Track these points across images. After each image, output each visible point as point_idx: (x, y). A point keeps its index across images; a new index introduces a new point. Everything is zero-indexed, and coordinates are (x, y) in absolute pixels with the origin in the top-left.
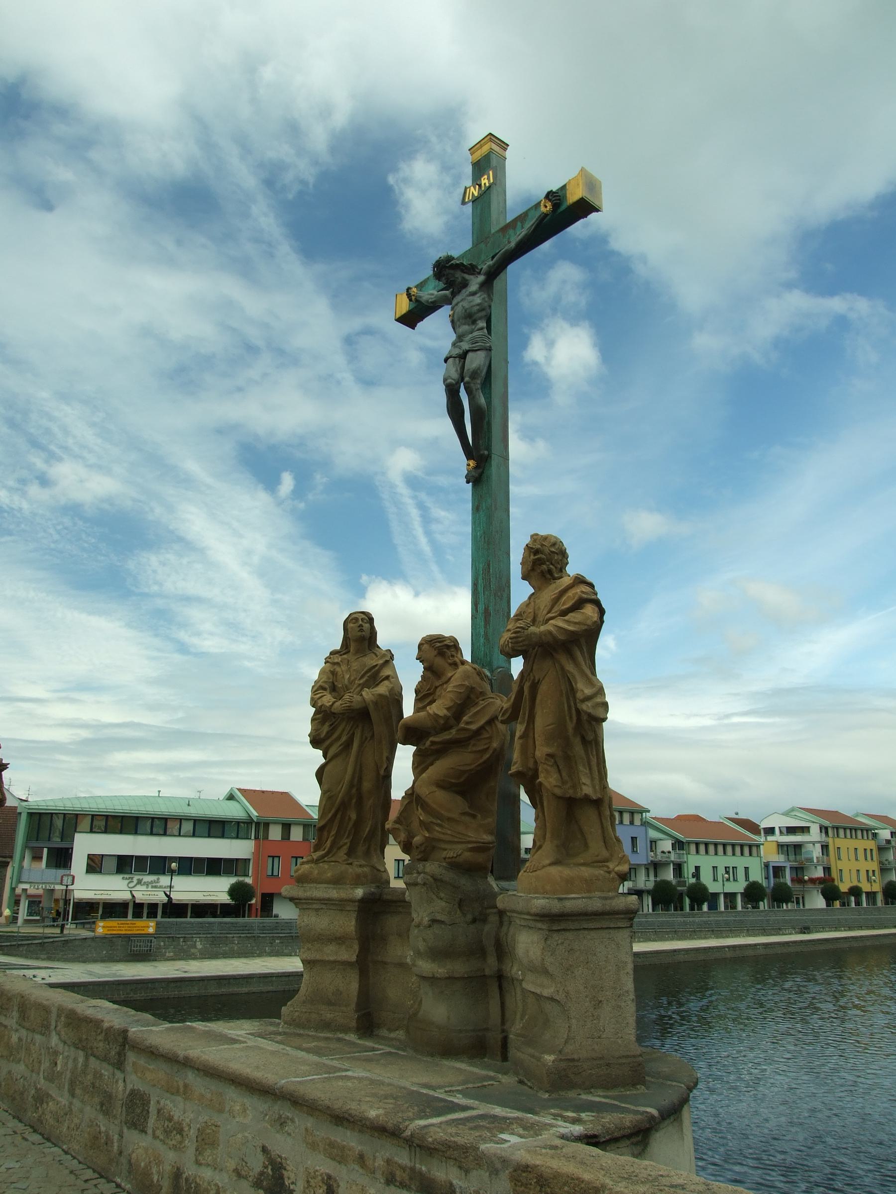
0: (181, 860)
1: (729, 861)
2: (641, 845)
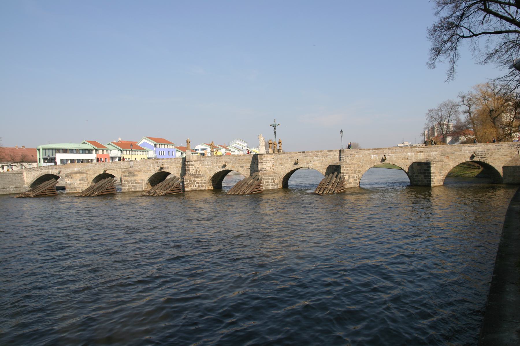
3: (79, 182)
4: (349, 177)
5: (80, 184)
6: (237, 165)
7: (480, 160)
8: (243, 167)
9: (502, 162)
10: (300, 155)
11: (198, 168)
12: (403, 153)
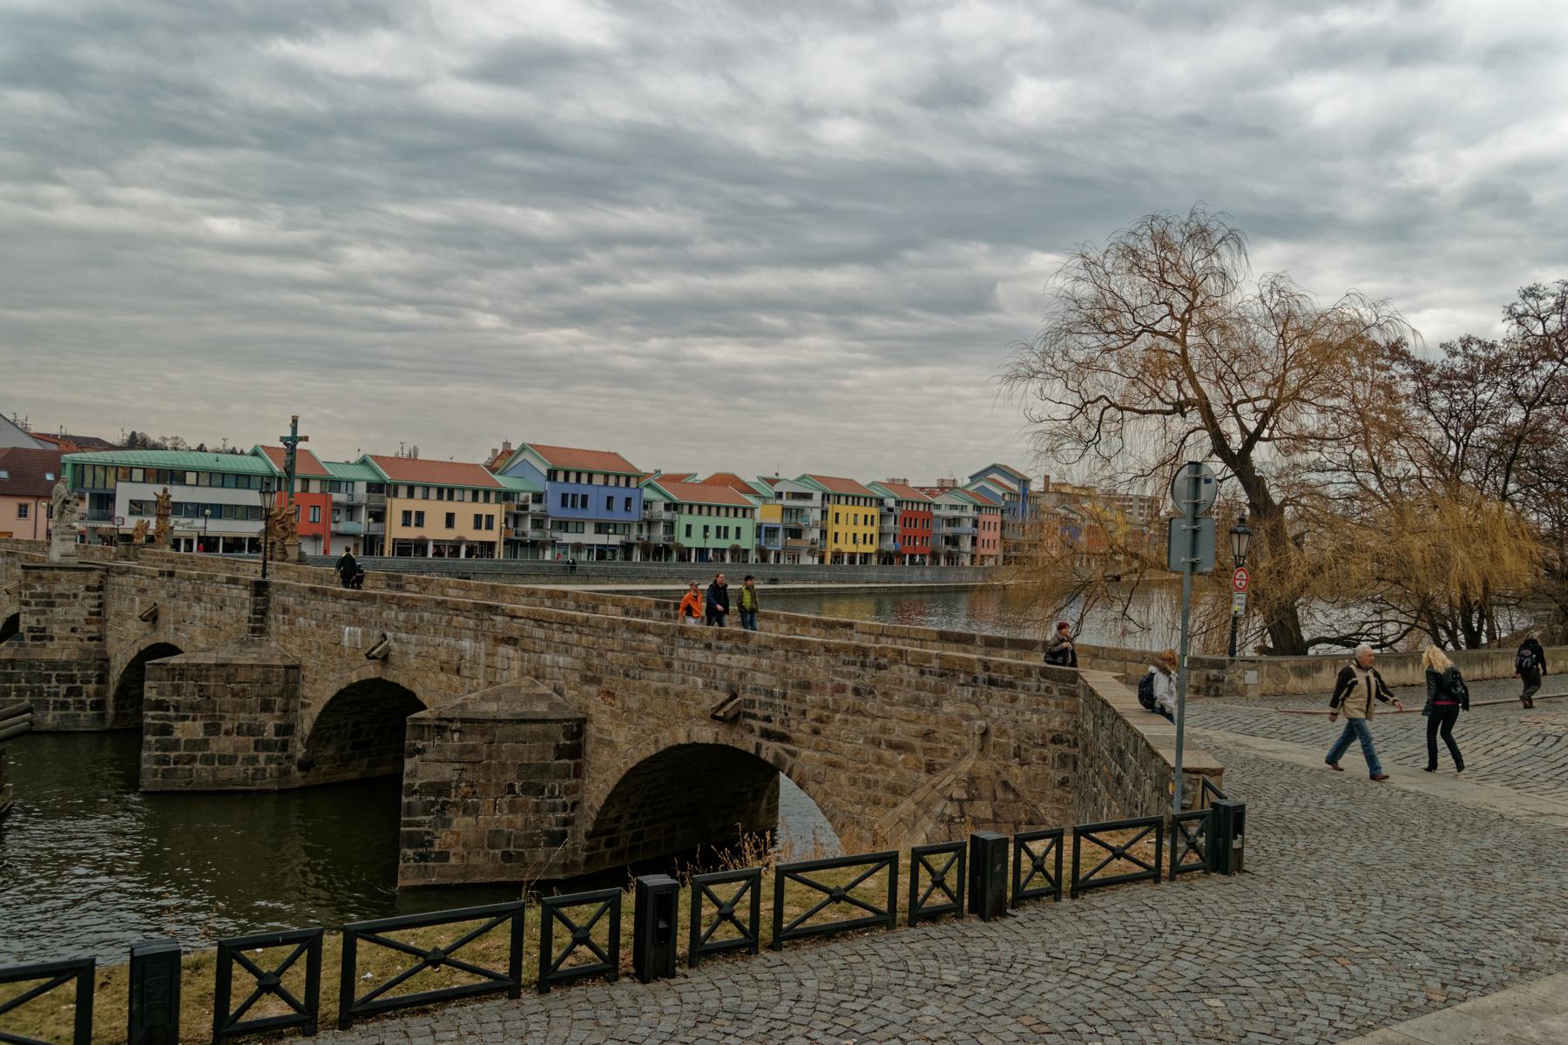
0: (211, 506)
1: (723, 521)
2: (635, 504)
4: (213, 729)
7: (758, 746)
9: (880, 793)
10: (163, 587)
12: (446, 635)
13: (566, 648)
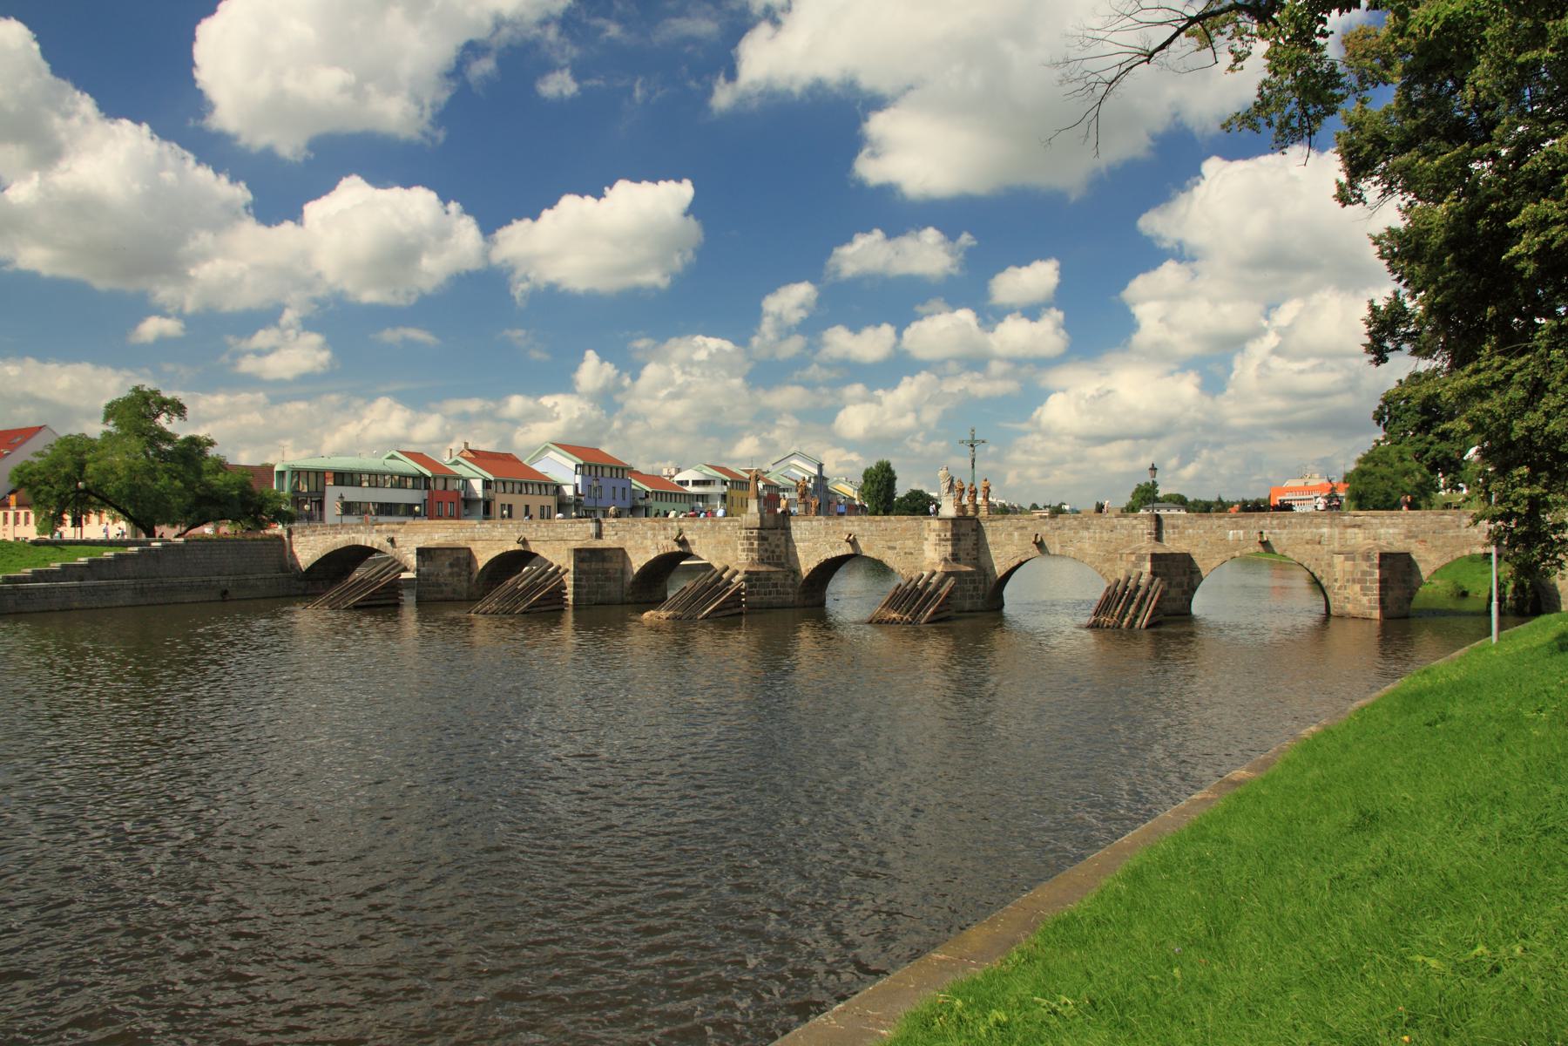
3: (447, 571)
5: (451, 574)
6: (880, 544)
8: (894, 548)
10: (1046, 524)
11: (777, 546)
13: (1395, 525)
